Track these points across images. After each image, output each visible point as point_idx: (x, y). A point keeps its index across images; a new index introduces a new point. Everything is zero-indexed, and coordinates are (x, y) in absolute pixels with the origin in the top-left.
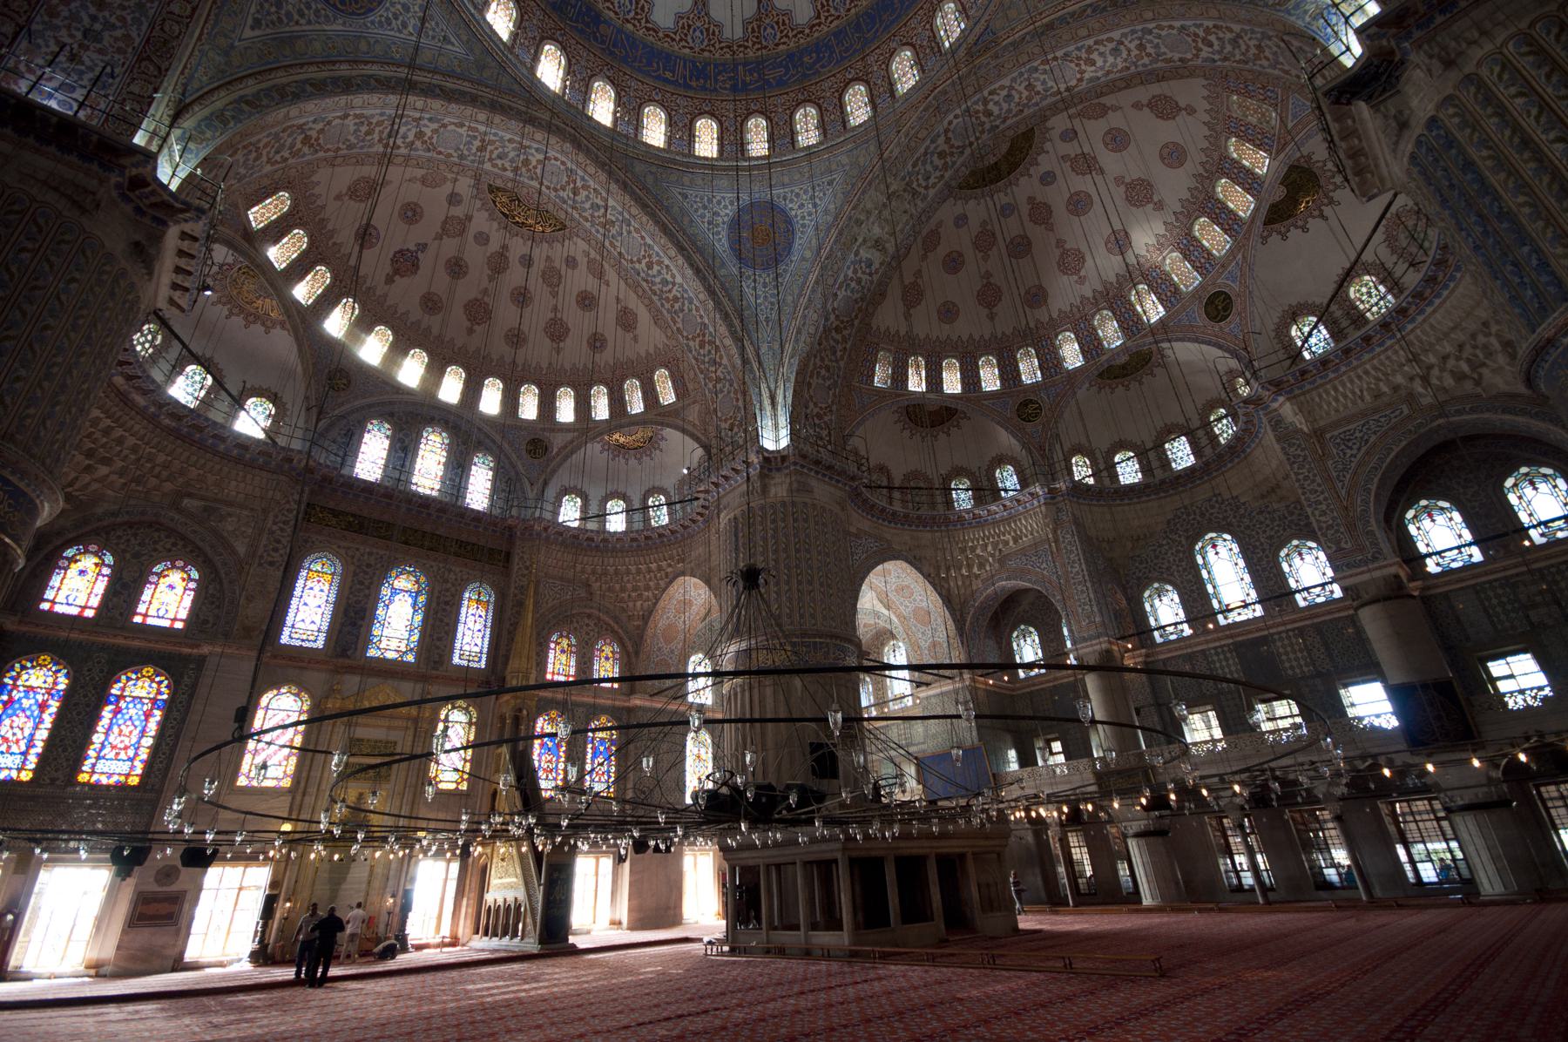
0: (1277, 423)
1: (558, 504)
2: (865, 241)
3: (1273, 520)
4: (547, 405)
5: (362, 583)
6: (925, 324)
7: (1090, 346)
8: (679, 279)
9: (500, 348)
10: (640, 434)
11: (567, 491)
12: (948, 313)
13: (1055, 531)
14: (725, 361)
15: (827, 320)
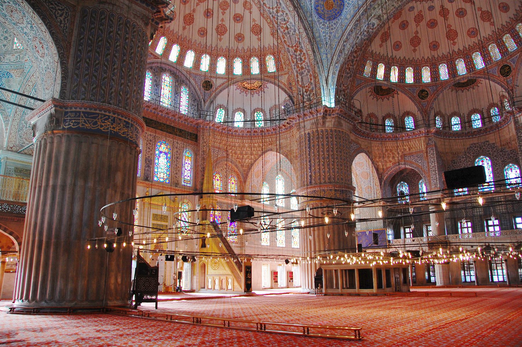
0: (516, 122)
1: (215, 112)
2: (374, 16)
3: (505, 155)
4: (213, 65)
5: (149, 148)
6: (387, 50)
7: (453, 71)
8: (291, 20)
9: (196, 38)
10: (256, 84)
11: (220, 106)
12: (397, 46)
13: (427, 148)
14: (307, 61)
15: (353, 48)
